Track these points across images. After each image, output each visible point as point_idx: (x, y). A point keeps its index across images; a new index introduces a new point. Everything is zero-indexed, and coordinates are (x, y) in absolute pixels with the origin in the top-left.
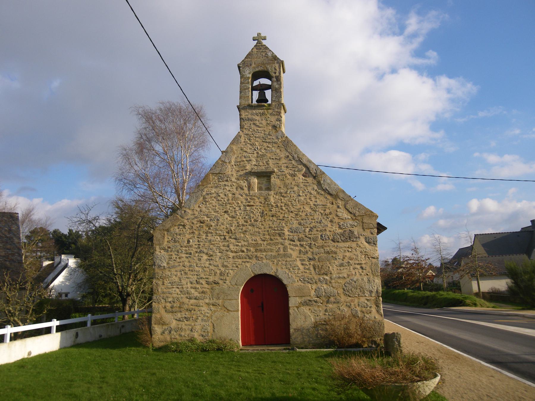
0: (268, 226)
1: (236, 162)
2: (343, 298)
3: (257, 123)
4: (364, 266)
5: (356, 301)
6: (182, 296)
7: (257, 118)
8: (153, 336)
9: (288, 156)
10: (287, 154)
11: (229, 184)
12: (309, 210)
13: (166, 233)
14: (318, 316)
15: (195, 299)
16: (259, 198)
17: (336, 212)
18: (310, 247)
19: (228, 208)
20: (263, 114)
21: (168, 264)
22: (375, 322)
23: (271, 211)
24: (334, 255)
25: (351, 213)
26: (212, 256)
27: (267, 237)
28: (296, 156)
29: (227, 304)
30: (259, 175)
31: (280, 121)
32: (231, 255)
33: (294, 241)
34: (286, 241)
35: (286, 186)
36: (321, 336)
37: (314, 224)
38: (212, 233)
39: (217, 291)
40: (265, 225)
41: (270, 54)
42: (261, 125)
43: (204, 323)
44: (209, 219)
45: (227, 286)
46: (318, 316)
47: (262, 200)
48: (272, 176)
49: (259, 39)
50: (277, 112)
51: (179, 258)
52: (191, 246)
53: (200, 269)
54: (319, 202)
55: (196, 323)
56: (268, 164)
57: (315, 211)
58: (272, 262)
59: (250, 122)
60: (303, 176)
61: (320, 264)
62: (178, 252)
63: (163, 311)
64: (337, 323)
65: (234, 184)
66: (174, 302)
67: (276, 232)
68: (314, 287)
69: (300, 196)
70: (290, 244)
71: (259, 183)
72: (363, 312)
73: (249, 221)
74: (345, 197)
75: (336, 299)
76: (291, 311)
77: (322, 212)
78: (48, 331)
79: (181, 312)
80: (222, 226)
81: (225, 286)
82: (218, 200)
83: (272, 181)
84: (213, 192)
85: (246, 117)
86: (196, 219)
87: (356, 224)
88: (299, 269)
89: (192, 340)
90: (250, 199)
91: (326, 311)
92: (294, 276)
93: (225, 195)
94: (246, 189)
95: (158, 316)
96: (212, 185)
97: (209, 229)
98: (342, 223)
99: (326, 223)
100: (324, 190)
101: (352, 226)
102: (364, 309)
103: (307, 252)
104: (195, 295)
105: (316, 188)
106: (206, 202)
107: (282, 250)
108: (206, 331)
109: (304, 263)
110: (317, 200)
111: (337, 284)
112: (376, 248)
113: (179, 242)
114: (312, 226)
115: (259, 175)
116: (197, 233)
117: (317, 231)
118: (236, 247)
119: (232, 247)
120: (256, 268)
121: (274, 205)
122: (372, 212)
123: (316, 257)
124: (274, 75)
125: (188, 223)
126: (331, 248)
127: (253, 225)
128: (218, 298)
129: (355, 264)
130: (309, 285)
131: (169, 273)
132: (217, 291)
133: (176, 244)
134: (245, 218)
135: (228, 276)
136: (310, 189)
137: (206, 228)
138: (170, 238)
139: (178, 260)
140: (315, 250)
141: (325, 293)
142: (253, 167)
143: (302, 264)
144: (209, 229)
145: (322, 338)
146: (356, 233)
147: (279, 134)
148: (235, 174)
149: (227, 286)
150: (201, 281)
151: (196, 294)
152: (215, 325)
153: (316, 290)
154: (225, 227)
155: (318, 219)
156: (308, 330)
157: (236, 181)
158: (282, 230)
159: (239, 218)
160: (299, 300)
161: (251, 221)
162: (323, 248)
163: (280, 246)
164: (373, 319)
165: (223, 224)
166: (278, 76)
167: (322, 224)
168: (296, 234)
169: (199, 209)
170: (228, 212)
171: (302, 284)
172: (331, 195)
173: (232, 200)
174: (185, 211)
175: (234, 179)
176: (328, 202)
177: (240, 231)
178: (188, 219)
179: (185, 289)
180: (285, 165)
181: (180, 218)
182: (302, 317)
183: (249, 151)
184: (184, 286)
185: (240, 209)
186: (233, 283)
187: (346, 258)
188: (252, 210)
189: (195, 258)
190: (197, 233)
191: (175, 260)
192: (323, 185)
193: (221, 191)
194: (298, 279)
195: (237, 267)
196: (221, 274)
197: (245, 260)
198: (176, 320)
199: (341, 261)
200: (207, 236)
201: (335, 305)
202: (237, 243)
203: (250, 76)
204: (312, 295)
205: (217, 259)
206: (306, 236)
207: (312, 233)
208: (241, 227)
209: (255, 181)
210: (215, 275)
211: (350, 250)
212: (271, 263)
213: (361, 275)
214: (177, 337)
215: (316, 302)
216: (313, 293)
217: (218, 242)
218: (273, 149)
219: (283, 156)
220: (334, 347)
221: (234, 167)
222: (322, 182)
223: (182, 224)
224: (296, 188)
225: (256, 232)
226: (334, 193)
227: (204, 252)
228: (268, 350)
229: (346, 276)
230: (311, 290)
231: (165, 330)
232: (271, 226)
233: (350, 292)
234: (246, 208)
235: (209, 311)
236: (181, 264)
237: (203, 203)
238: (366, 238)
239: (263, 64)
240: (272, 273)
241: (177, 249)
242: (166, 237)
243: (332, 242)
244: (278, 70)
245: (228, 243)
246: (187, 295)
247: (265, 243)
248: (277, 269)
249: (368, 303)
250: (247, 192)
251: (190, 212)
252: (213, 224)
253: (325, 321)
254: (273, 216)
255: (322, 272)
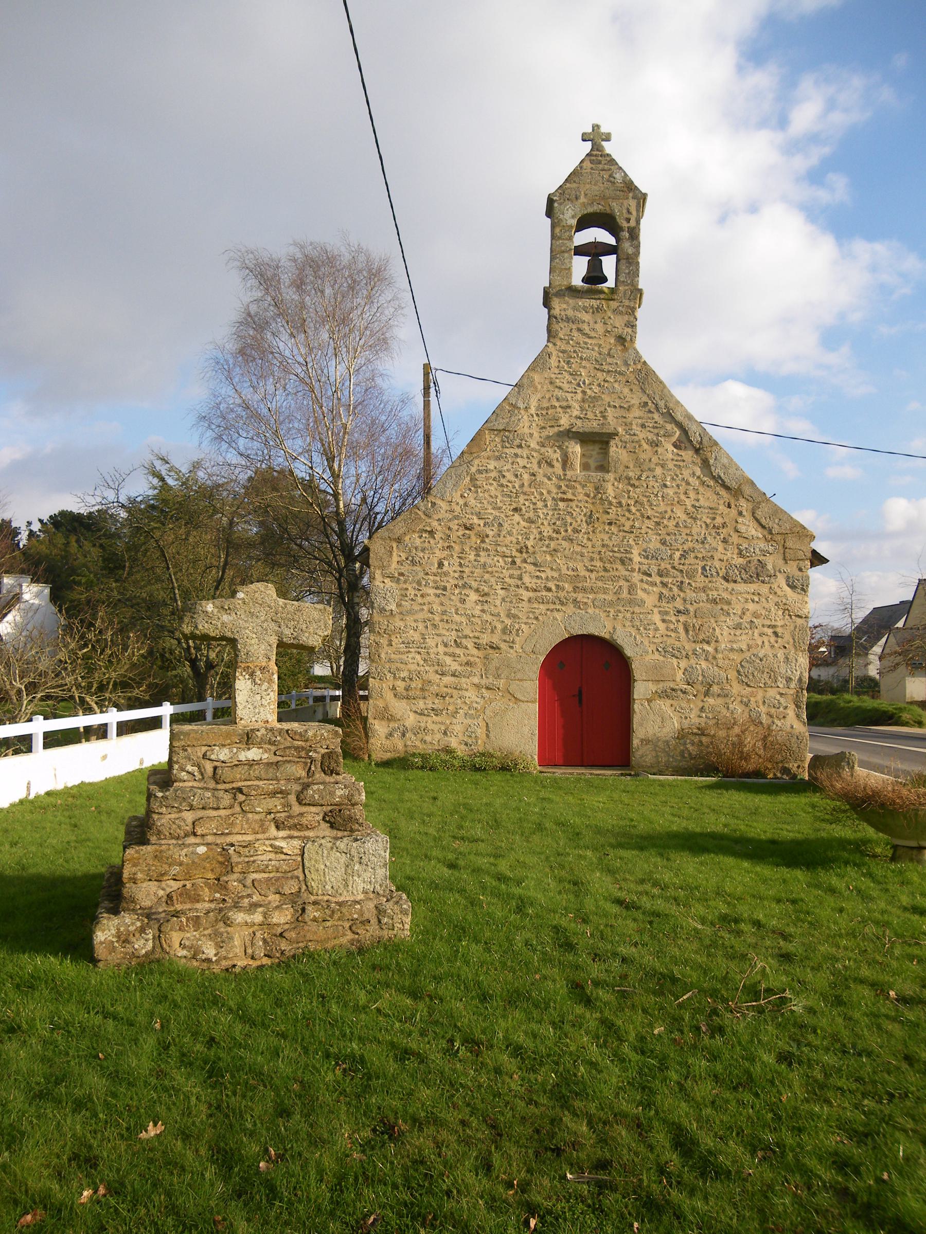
0: (600, 543)
1: (539, 408)
2: (736, 688)
3: (586, 327)
4: (779, 630)
5: (760, 694)
6: (427, 668)
7: (586, 317)
8: (372, 741)
9: (646, 404)
10: (645, 399)
11: (525, 452)
12: (684, 517)
13: (395, 545)
14: (686, 718)
15: (453, 675)
16: (584, 486)
17: (735, 524)
18: (681, 589)
19: (522, 501)
20: (598, 309)
21: (399, 605)
22: (790, 735)
23: (608, 513)
24: (725, 607)
25: (763, 527)
26: (486, 594)
27: (598, 564)
28: (661, 404)
29: (513, 688)
30: (585, 438)
31: (633, 326)
32: (526, 595)
33: (650, 575)
34: (635, 574)
35: (639, 464)
36: (690, 754)
37: (690, 544)
38: (487, 550)
39: (495, 663)
40: (594, 540)
41: (618, 176)
42: (593, 334)
43: (468, 721)
44: (482, 522)
45: (515, 654)
46: (686, 718)
47: (590, 489)
48: (612, 443)
49: (596, 137)
50: (628, 307)
51: (422, 596)
52: (446, 574)
53: (464, 619)
54: (702, 502)
55: (454, 721)
56: (604, 417)
57: (695, 519)
58: (605, 614)
59: (571, 325)
60: (675, 446)
61: (698, 623)
62: (419, 583)
63: (389, 695)
64: (722, 733)
65: (535, 454)
66: (411, 679)
67: (616, 555)
68: (684, 664)
69: (665, 486)
70: (642, 581)
71: (583, 455)
72: (771, 716)
73: (562, 530)
74: (755, 495)
75: (722, 689)
76: (637, 707)
77: (708, 521)
78: (154, 723)
79: (424, 698)
80: (509, 538)
81: (512, 654)
82: (502, 485)
83: (611, 454)
84: (491, 467)
85: (563, 313)
86: (456, 522)
87: (771, 549)
88: (657, 629)
89: (448, 751)
90: (567, 486)
91: (702, 709)
92: (646, 643)
93: (516, 476)
94: (558, 465)
95: (381, 704)
96: (490, 454)
97: (483, 542)
98: (745, 545)
99: (714, 545)
100: (714, 477)
101: (764, 553)
102: (773, 711)
103: (674, 598)
104: (453, 668)
105: (698, 472)
106: (476, 486)
107: (625, 591)
108: (473, 735)
109: (667, 618)
110: (700, 497)
111: (727, 662)
112: (806, 599)
113: (421, 564)
114: (686, 547)
115: (585, 438)
116: (457, 548)
117: (696, 558)
118: (535, 580)
119: (526, 579)
120: (573, 623)
121: (614, 501)
122: (805, 528)
123: (691, 609)
124: (625, 224)
125: (439, 528)
126: (720, 592)
127: (571, 540)
128: (498, 677)
129: (763, 626)
130: (675, 660)
131: (402, 624)
132: (495, 663)
133: (415, 568)
134: (554, 524)
135: (518, 636)
136: (686, 473)
137: (475, 540)
138: (404, 556)
139: (419, 600)
140: (690, 595)
141: (704, 676)
142: (573, 421)
143: (664, 621)
144: (483, 542)
145: (691, 759)
146: (770, 567)
147: (631, 355)
148: (536, 435)
149: (515, 654)
150: (464, 641)
151: (455, 666)
152: (490, 725)
153: (685, 669)
154: (515, 541)
155: (699, 534)
156: (667, 742)
157: (538, 447)
158: (627, 552)
159: (542, 524)
160: (652, 687)
161: (566, 531)
162: (704, 591)
163: (622, 583)
164: (789, 729)
165: (510, 533)
166: (634, 228)
167: (707, 546)
168: (654, 561)
169: (461, 502)
170: (521, 509)
171: (662, 658)
172: (727, 488)
173: (530, 486)
174: (434, 504)
175: (533, 445)
176: (721, 502)
177: (544, 549)
178: (439, 520)
179: (432, 656)
180: (640, 421)
181: (423, 516)
182: (655, 720)
183: (566, 386)
184: (431, 651)
185: (546, 506)
186: (528, 649)
187: (748, 613)
188: (569, 509)
189: (453, 597)
190: (457, 548)
191: (412, 600)
192: (713, 469)
193: (509, 466)
194: (653, 647)
195: (537, 618)
196: (504, 631)
197: (552, 607)
198: (416, 712)
199: (737, 619)
200: (478, 555)
201: (720, 701)
202: (538, 573)
203: (574, 222)
204: (678, 679)
205: (498, 603)
206: (674, 568)
207: (687, 562)
208: (547, 542)
209: (576, 449)
210: (492, 632)
211: (756, 599)
212: (603, 615)
213: (773, 646)
214: (418, 743)
215: (684, 693)
216: (680, 675)
217: (499, 570)
218: (616, 385)
219: (635, 401)
220: (716, 775)
221: (536, 418)
222: (712, 462)
223: (429, 529)
224: (659, 471)
225: (577, 554)
226: (734, 485)
227: (470, 587)
228: (591, 774)
229: (744, 647)
230: (677, 670)
231: (394, 730)
232: (605, 542)
233: (751, 677)
234: (557, 505)
235: (478, 700)
236: (425, 608)
237: (470, 490)
238: (788, 577)
239: (604, 198)
240: (604, 633)
241: (416, 578)
242: (394, 554)
243: (723, 582)
244: (634, 213)
245: (519, 572)
246: (436, 667)
247: (593, 576)
248: (614, 628)
249: (782, 700)
250: (561, 472)
251: (444, 505)
252: (491, 533)
253: (699, 729)
254: (610, 524)
255: (701, 637)
